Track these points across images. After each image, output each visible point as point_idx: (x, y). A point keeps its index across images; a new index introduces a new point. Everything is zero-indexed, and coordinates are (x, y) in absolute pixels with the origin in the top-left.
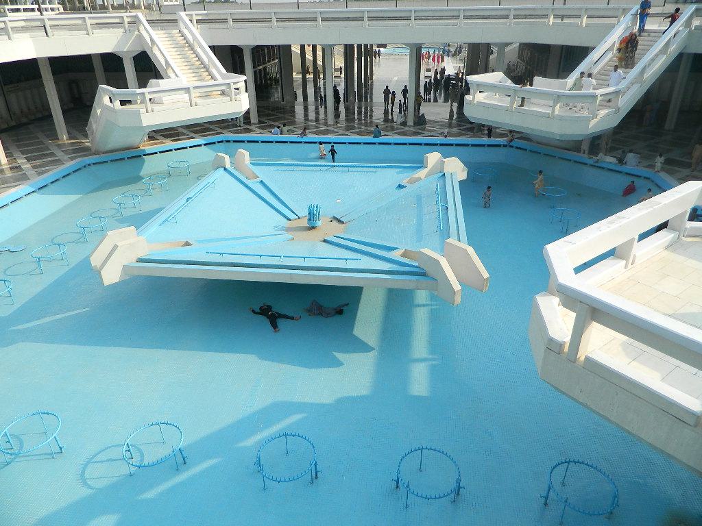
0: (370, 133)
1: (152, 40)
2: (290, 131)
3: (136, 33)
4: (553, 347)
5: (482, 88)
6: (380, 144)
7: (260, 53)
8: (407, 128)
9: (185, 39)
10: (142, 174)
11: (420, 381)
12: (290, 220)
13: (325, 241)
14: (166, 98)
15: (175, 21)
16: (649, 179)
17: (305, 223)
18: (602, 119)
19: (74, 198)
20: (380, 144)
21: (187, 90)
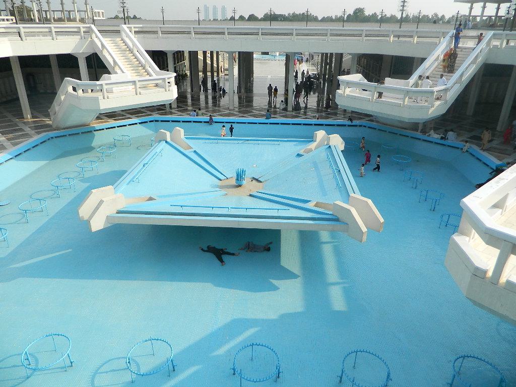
0: (262, 116)
1: (103, 45)
3: (90, 39)
4: (478, 273)
5: (349, 84)
6: (270, 124)
7: (178, 55)
8: (288, 113)
10: (92, 145)
11: (337, 299)
12: (221, 180)
13: (251, 195)
14: (115, 89)
15: (118, 32)
17: (233, 182)
18: (436, 108)
19: (42, 163)
20: (270, 124)
21: (134, 82)
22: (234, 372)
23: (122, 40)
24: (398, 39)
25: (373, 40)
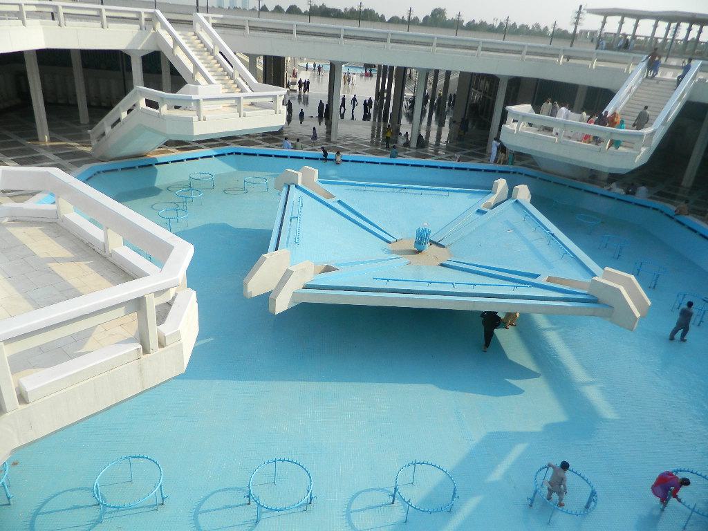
1: (176, 42)
2: (302, 148)
3: (152, 31)
6: (397, 164)
9: (201, 43)
10: (156, 185)
12: (389, 243)
13: (442, 265)
15: (190, 23)
16: (657, 209)
20: (397, 164)
22: (532, 503)
23: (195, 35)
24: (568, 60)
25: (535, 60)
